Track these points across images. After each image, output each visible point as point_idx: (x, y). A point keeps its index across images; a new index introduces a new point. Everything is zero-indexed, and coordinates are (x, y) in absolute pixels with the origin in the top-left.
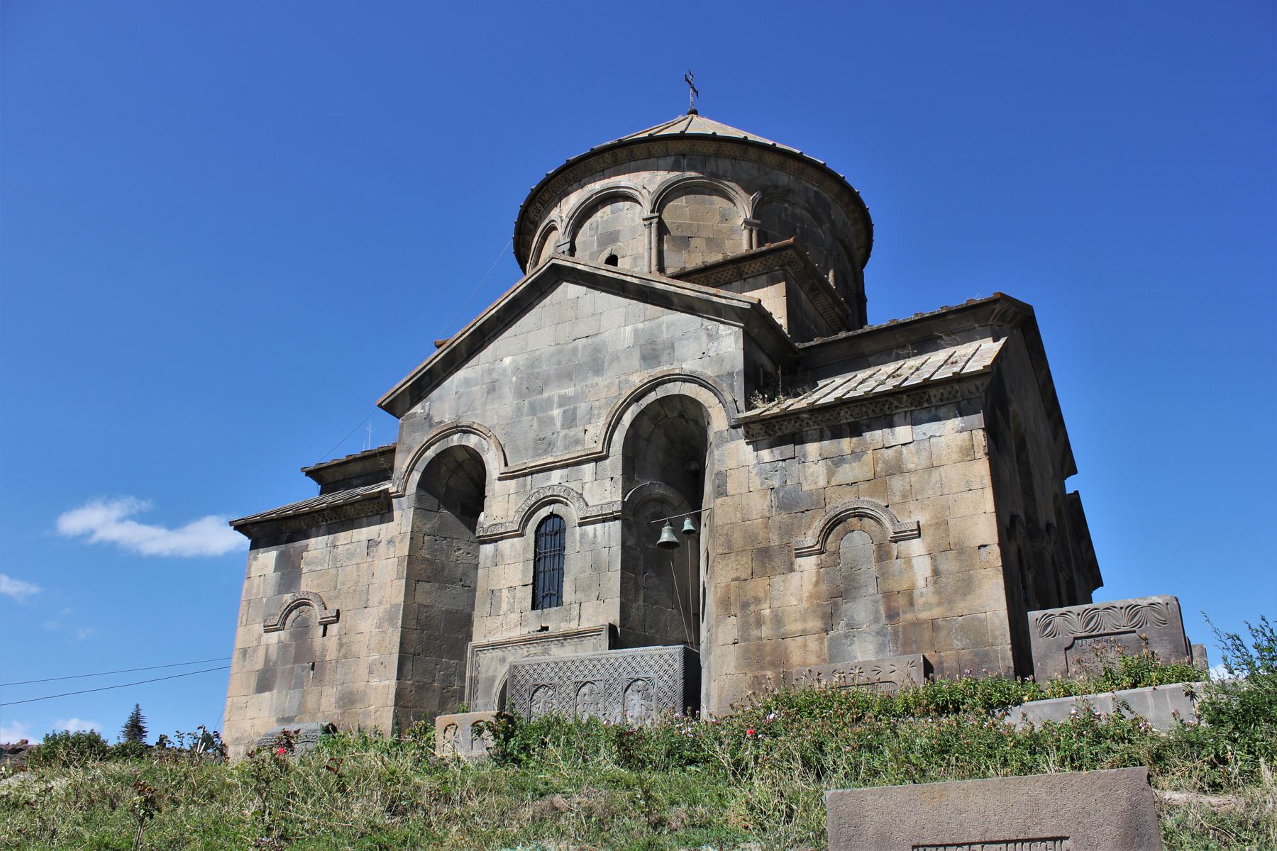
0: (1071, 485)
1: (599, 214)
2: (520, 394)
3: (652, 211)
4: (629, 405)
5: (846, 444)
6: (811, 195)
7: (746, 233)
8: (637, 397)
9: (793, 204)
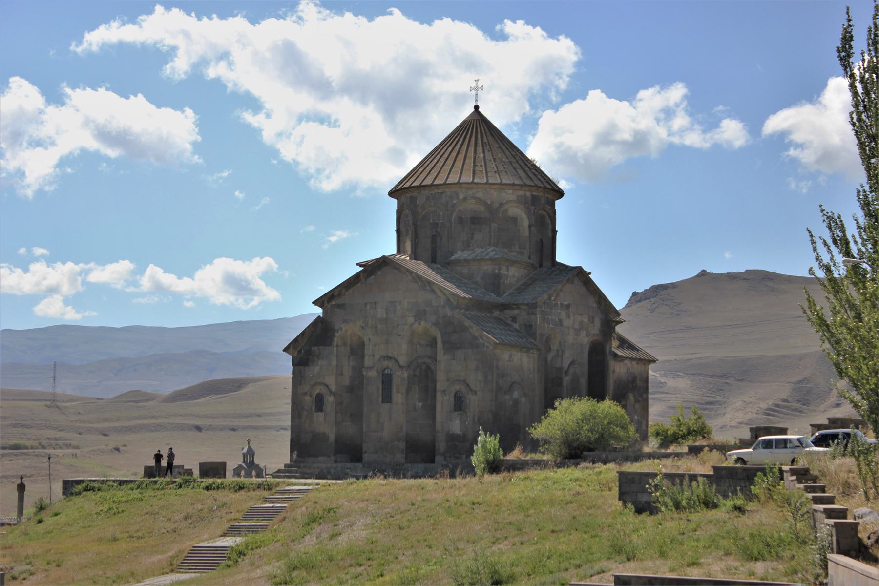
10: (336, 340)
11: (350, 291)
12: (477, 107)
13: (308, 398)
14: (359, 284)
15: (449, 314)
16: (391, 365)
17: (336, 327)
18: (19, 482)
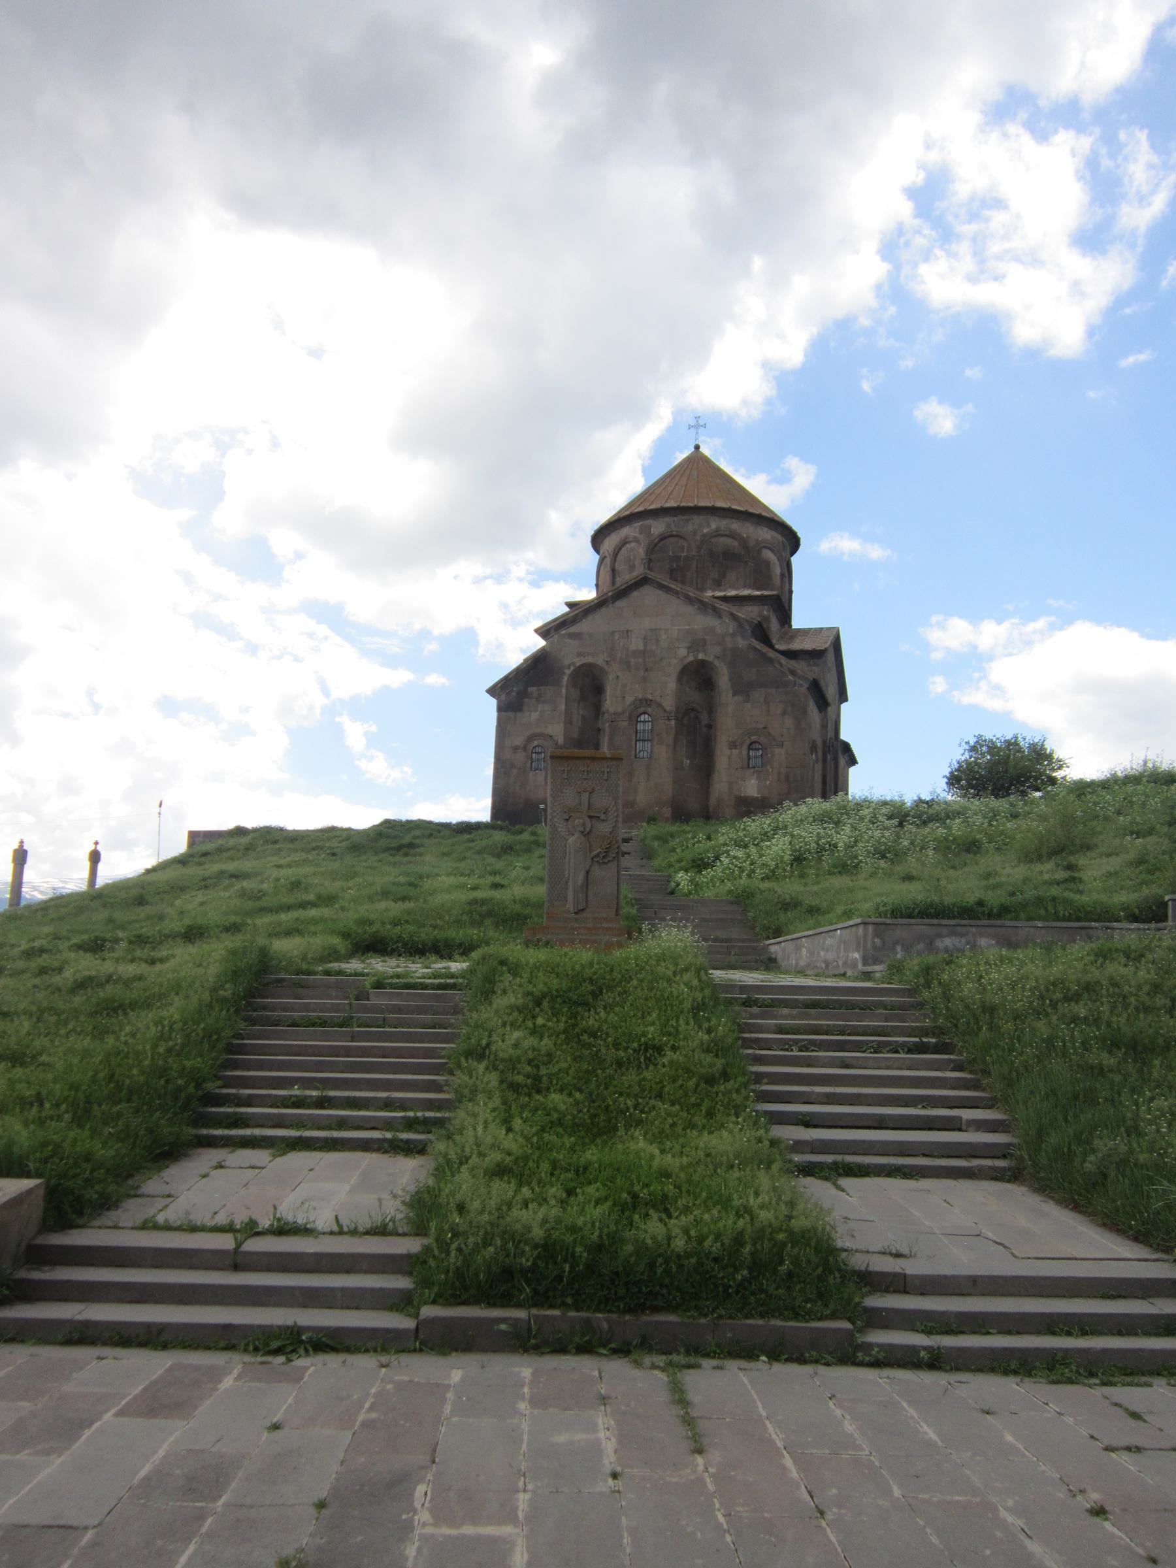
10: (566, 678)
11: (590, 618)
12: (697, 447)
15: (741, 643)
16: (649, 710)
18: (93, 847)
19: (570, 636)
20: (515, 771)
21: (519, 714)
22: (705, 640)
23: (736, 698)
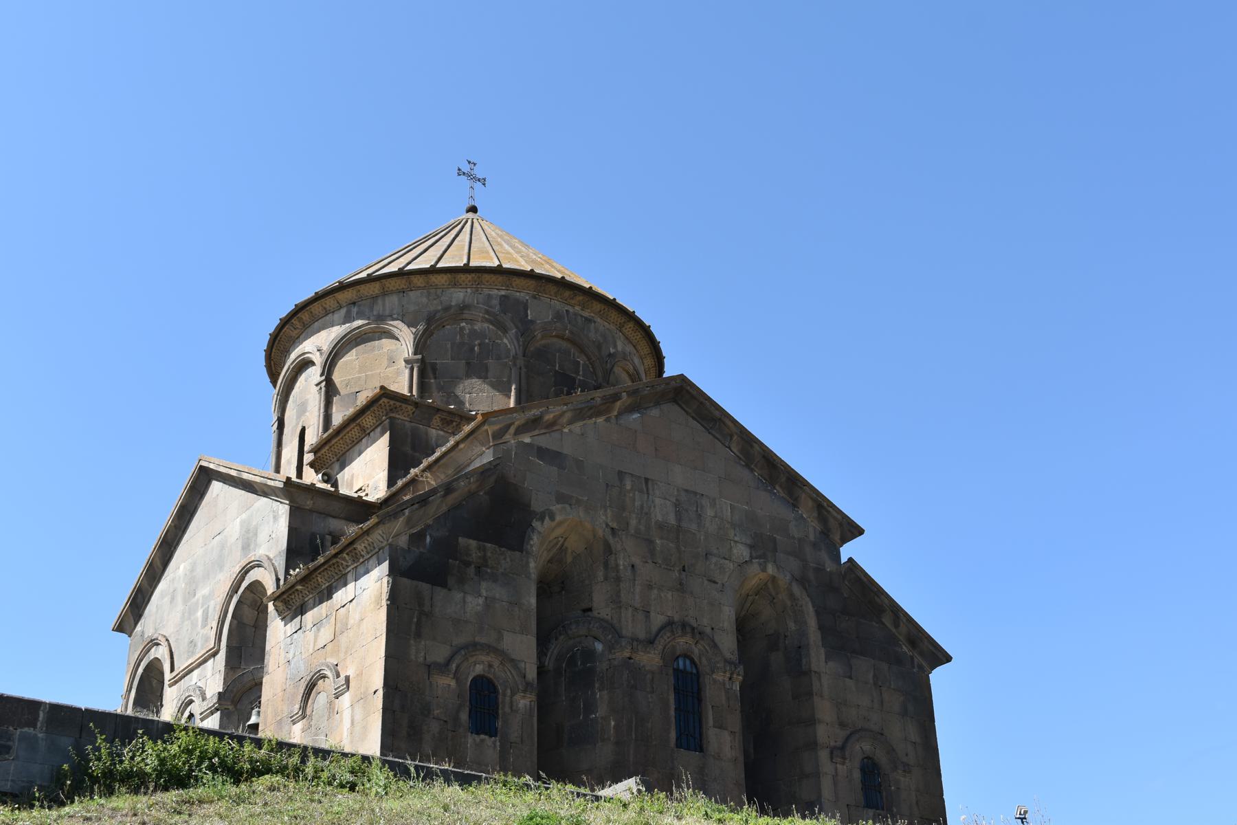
0: (847, 551)
1: (298, 384)
2: (185, 601)
3: (322, 375)
4: (231, 597)
5: (323, 609)
6: (495, 302)
7: (407, 372)
8: (235, 589)
9: (471, 321)
11: (577, 427)
13: (445, 682)
14: (600, 420)
16: (696, 651)
17: (537, 505)
19: (542, 453)
20: (435, 727)
21: (440, 593)
22: (774, 541)
23: (831, 664)
